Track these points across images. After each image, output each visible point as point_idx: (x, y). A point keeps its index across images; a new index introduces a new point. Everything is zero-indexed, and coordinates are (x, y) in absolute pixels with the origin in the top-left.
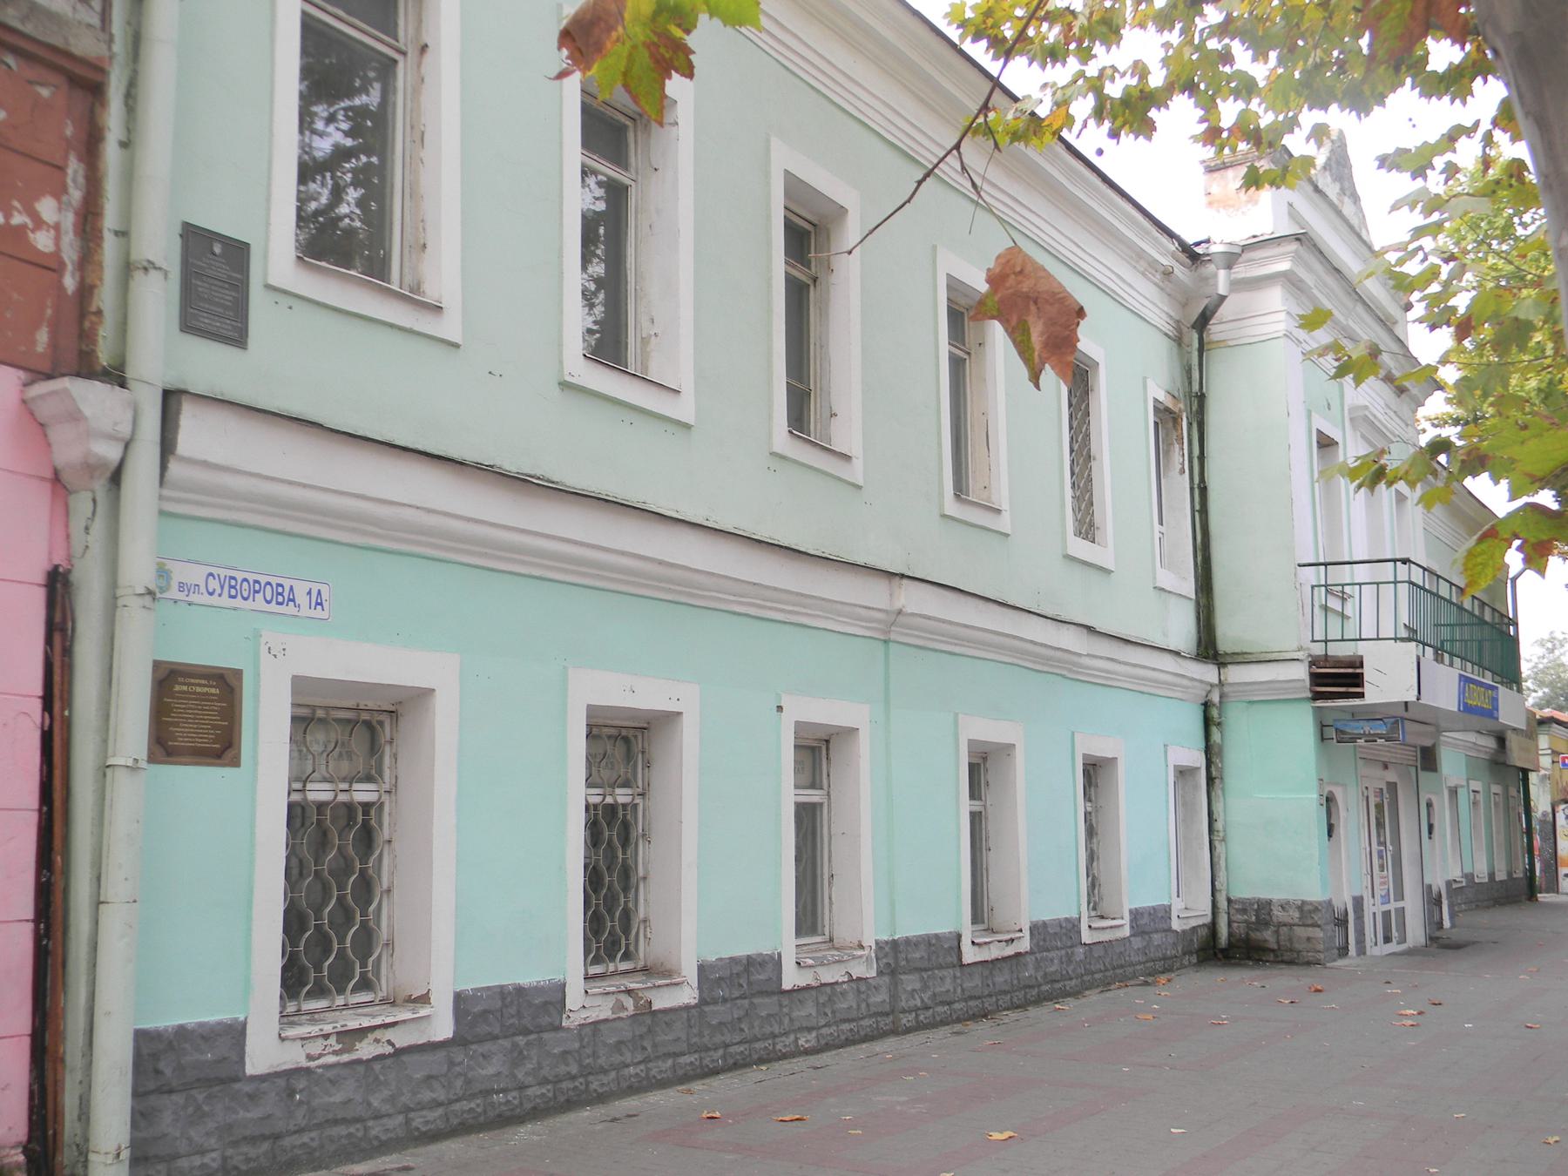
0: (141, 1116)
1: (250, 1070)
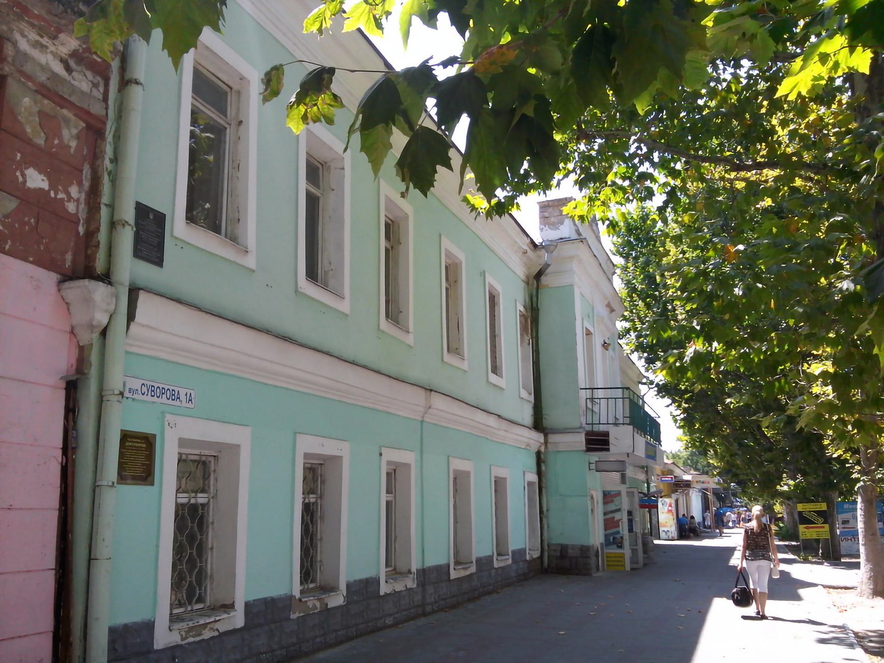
1: (156, 647)
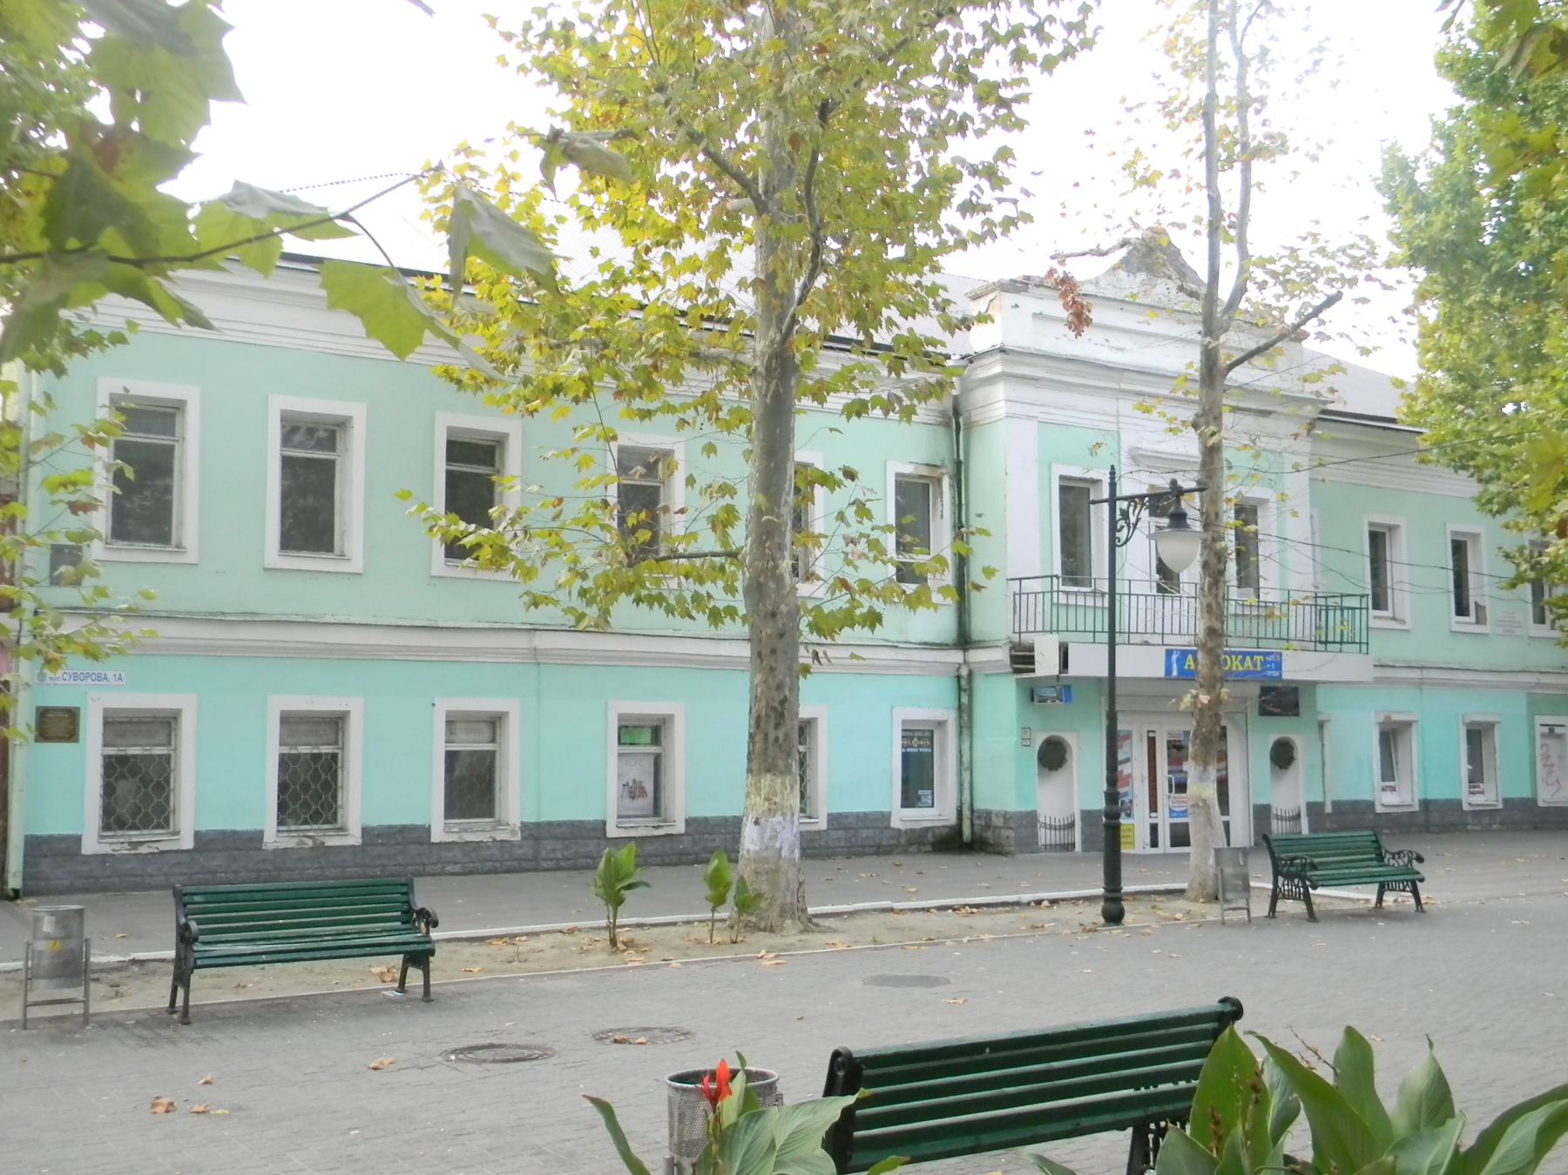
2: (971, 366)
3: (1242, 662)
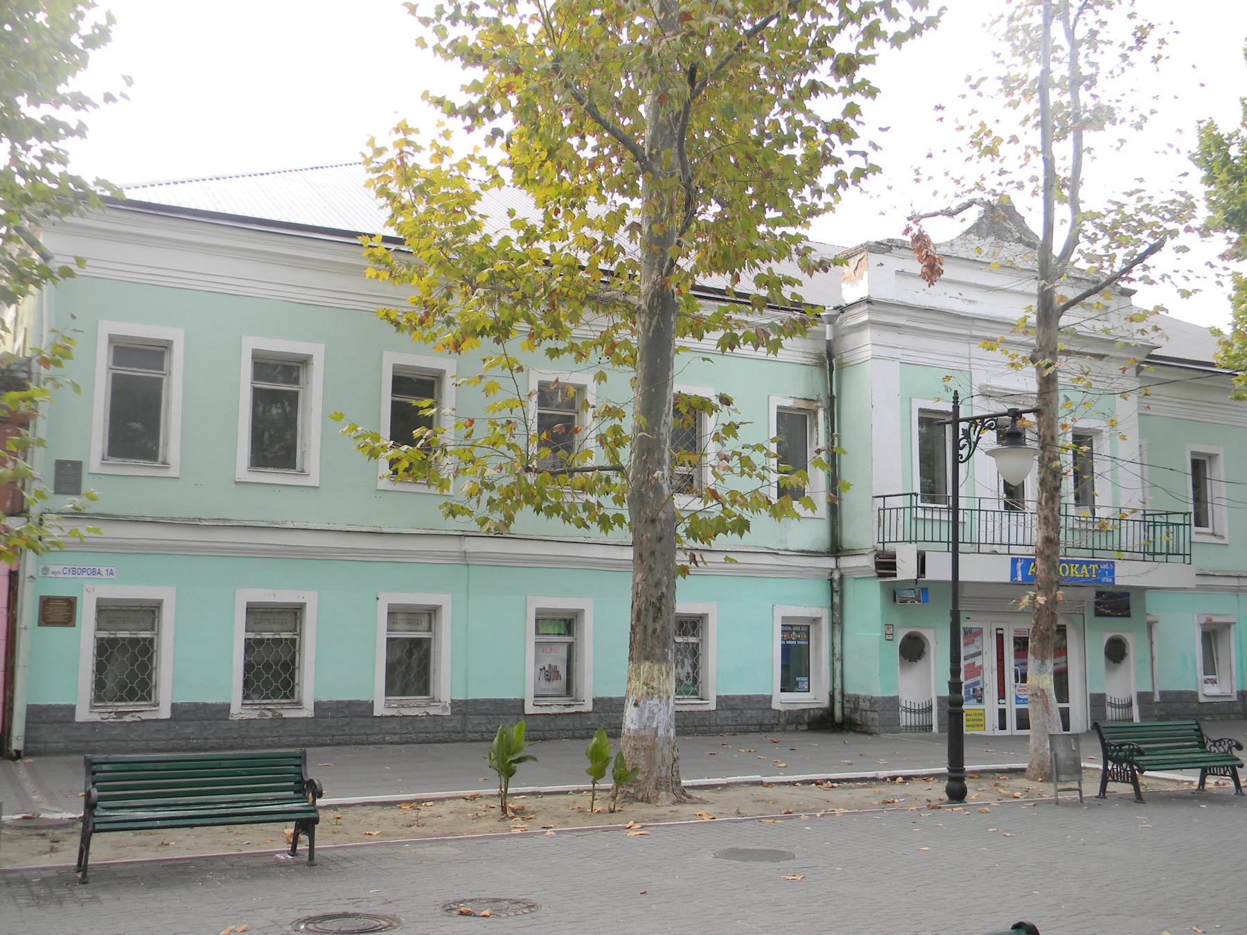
0: (27, 728)
1: (77, 720)
2: (842, 316)
3: (1079, 570)
